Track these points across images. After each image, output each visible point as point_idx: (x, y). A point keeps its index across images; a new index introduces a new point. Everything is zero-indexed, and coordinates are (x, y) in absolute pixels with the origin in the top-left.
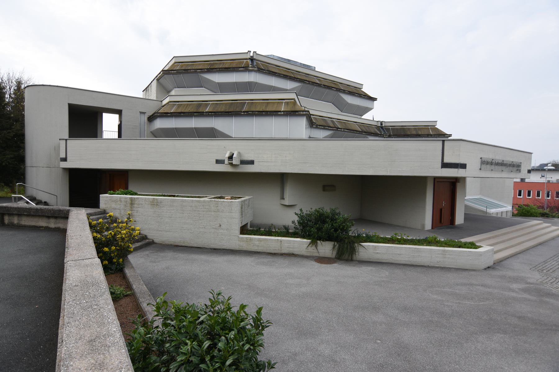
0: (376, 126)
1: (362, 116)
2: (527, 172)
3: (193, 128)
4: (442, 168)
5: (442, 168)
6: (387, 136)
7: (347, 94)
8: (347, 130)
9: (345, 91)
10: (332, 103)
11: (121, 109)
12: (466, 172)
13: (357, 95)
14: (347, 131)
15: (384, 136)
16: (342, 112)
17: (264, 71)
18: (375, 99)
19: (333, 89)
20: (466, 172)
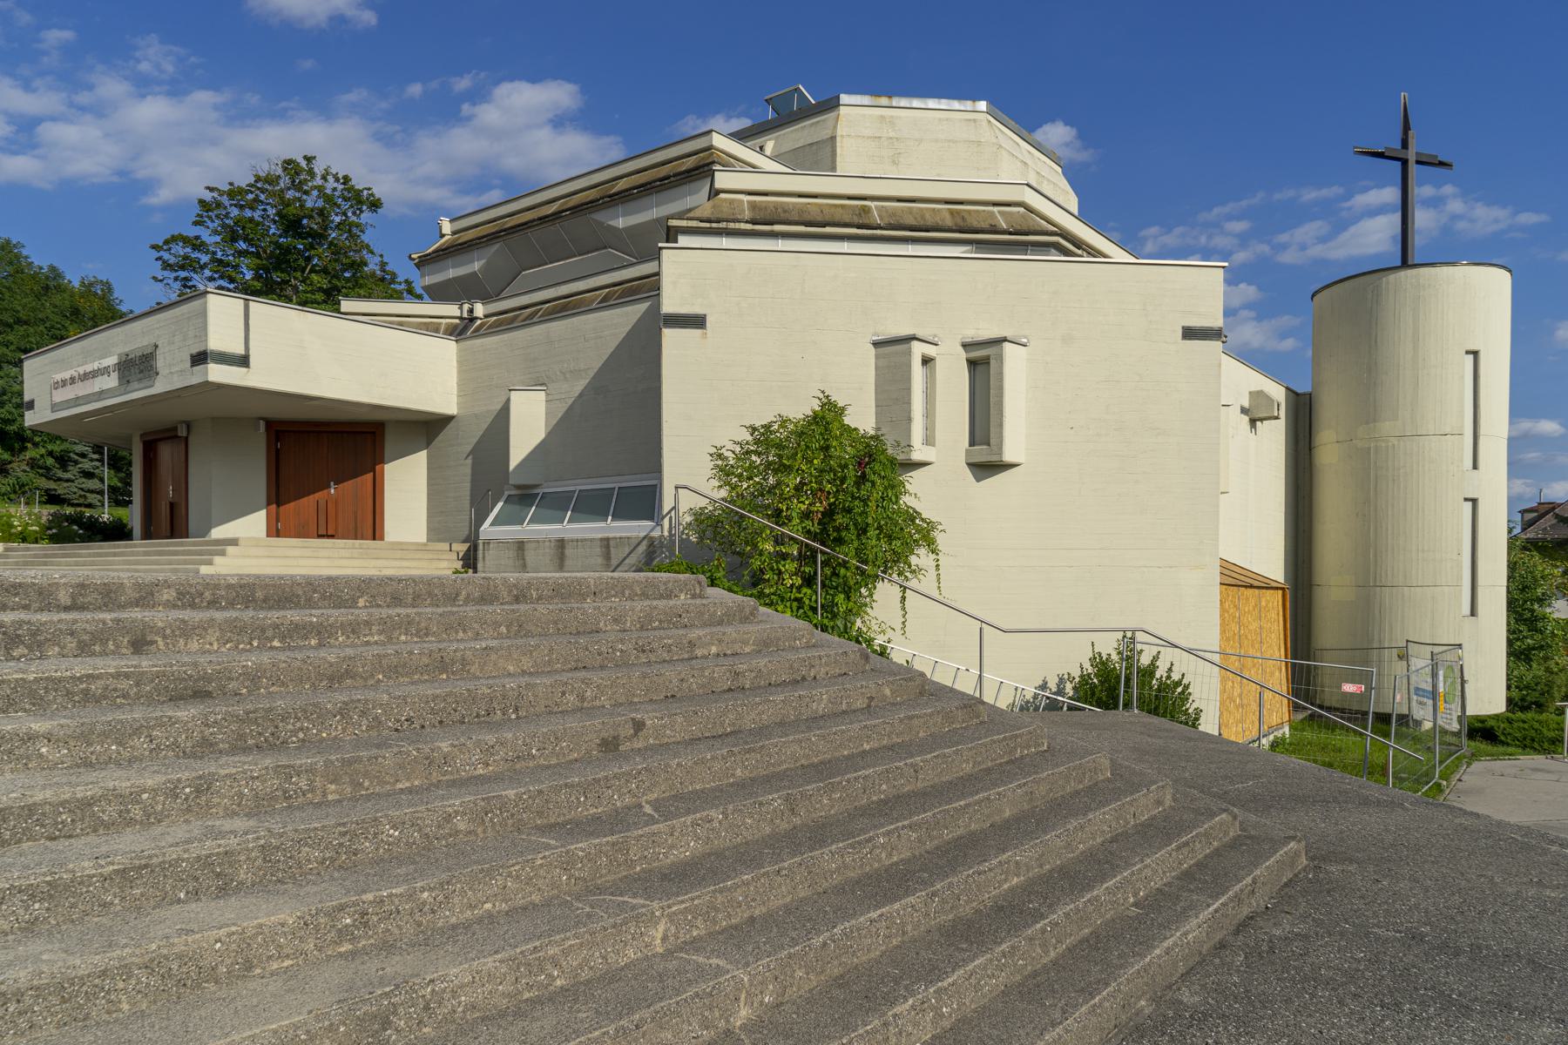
9: (597, 203)
13: (635, 191)
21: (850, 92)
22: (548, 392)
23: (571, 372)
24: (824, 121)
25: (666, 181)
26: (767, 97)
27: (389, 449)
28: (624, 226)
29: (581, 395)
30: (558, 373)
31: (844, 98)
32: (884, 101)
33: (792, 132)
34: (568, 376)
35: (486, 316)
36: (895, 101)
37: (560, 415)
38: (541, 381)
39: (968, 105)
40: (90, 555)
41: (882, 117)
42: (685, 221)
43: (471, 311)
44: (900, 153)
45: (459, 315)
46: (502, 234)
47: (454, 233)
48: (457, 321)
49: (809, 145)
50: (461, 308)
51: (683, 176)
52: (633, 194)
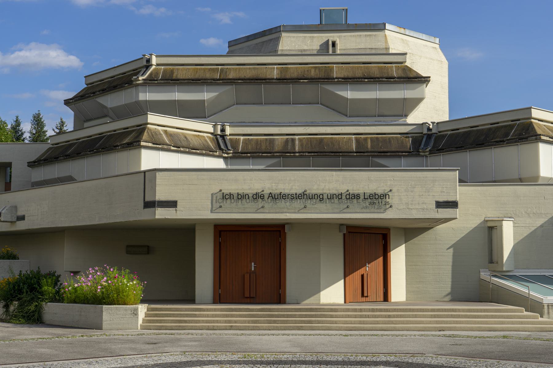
0: (422, 133)
1: (406, 116)
2: (434, 206)
3: (56, 178)
4: (144, 208)
5: (144, 208)
6: (427, 153)
7: (339, 83)
8: (309, 153)
9: (333, 80)
10: (321, 104)
11: (10, 161)
12: (176, 212)
13: (366, 80)
14: (309, 154)
15: (421, 154)
16: (347, 116)
17: (156, 82)
18: (423, 79)
19: (302, 81)
20: (176, 212)
21: (390, 23)
22: (515, 222)
23: (534, 213)
24: (375, 35)
25: (392, 80)
26: (321, 8)
27: (392, 242)
28: (351, 98)
29: (542, 226)
30: (523, 213)
31: (388, 26)
32: (402, 30)
33: (351, 36)
34: (531, 215)
35: (230, 135)
36: (407, 32)
37: (525, 235)
38: (510, 215)
39: (432, 39)
40: (222, 310)
41: (402, 40)
42: (545, 137)
43: (223, 130)
44: (413, 62)
45: (212, 131)
46: (239, 81)
47: (158, 65)
48: (210, 135)
49: (369, 48)
50: (215, 126)
51: (405, 80)
52: (364, 81)
